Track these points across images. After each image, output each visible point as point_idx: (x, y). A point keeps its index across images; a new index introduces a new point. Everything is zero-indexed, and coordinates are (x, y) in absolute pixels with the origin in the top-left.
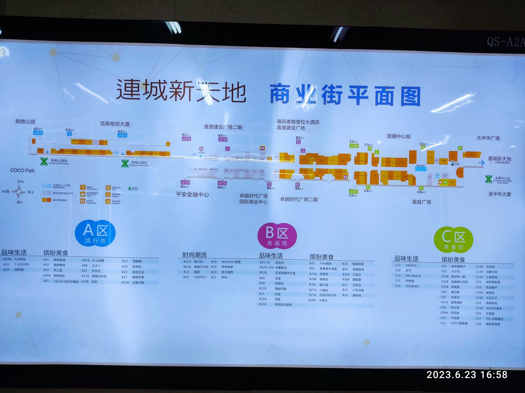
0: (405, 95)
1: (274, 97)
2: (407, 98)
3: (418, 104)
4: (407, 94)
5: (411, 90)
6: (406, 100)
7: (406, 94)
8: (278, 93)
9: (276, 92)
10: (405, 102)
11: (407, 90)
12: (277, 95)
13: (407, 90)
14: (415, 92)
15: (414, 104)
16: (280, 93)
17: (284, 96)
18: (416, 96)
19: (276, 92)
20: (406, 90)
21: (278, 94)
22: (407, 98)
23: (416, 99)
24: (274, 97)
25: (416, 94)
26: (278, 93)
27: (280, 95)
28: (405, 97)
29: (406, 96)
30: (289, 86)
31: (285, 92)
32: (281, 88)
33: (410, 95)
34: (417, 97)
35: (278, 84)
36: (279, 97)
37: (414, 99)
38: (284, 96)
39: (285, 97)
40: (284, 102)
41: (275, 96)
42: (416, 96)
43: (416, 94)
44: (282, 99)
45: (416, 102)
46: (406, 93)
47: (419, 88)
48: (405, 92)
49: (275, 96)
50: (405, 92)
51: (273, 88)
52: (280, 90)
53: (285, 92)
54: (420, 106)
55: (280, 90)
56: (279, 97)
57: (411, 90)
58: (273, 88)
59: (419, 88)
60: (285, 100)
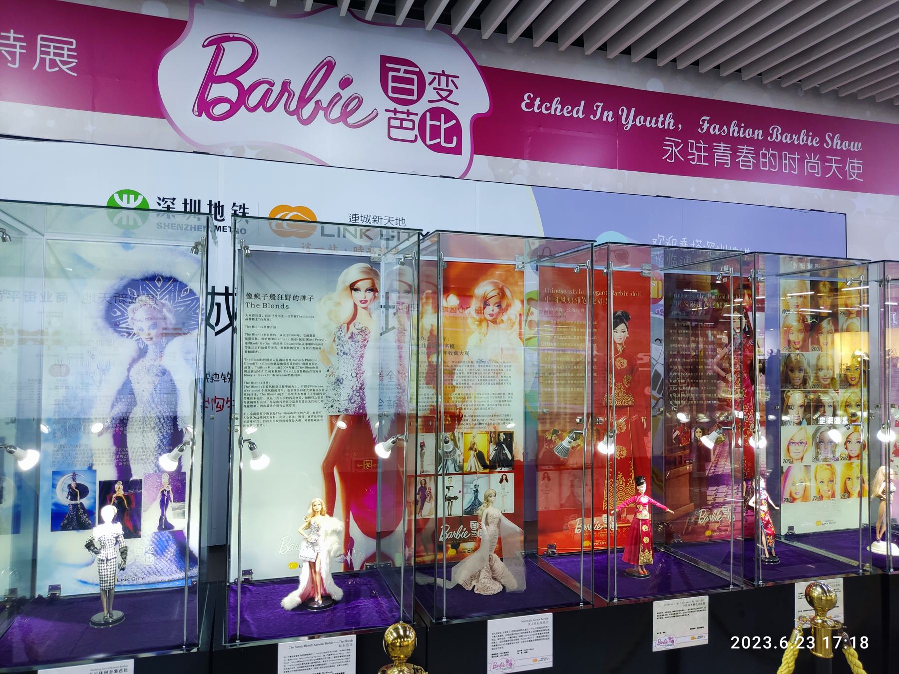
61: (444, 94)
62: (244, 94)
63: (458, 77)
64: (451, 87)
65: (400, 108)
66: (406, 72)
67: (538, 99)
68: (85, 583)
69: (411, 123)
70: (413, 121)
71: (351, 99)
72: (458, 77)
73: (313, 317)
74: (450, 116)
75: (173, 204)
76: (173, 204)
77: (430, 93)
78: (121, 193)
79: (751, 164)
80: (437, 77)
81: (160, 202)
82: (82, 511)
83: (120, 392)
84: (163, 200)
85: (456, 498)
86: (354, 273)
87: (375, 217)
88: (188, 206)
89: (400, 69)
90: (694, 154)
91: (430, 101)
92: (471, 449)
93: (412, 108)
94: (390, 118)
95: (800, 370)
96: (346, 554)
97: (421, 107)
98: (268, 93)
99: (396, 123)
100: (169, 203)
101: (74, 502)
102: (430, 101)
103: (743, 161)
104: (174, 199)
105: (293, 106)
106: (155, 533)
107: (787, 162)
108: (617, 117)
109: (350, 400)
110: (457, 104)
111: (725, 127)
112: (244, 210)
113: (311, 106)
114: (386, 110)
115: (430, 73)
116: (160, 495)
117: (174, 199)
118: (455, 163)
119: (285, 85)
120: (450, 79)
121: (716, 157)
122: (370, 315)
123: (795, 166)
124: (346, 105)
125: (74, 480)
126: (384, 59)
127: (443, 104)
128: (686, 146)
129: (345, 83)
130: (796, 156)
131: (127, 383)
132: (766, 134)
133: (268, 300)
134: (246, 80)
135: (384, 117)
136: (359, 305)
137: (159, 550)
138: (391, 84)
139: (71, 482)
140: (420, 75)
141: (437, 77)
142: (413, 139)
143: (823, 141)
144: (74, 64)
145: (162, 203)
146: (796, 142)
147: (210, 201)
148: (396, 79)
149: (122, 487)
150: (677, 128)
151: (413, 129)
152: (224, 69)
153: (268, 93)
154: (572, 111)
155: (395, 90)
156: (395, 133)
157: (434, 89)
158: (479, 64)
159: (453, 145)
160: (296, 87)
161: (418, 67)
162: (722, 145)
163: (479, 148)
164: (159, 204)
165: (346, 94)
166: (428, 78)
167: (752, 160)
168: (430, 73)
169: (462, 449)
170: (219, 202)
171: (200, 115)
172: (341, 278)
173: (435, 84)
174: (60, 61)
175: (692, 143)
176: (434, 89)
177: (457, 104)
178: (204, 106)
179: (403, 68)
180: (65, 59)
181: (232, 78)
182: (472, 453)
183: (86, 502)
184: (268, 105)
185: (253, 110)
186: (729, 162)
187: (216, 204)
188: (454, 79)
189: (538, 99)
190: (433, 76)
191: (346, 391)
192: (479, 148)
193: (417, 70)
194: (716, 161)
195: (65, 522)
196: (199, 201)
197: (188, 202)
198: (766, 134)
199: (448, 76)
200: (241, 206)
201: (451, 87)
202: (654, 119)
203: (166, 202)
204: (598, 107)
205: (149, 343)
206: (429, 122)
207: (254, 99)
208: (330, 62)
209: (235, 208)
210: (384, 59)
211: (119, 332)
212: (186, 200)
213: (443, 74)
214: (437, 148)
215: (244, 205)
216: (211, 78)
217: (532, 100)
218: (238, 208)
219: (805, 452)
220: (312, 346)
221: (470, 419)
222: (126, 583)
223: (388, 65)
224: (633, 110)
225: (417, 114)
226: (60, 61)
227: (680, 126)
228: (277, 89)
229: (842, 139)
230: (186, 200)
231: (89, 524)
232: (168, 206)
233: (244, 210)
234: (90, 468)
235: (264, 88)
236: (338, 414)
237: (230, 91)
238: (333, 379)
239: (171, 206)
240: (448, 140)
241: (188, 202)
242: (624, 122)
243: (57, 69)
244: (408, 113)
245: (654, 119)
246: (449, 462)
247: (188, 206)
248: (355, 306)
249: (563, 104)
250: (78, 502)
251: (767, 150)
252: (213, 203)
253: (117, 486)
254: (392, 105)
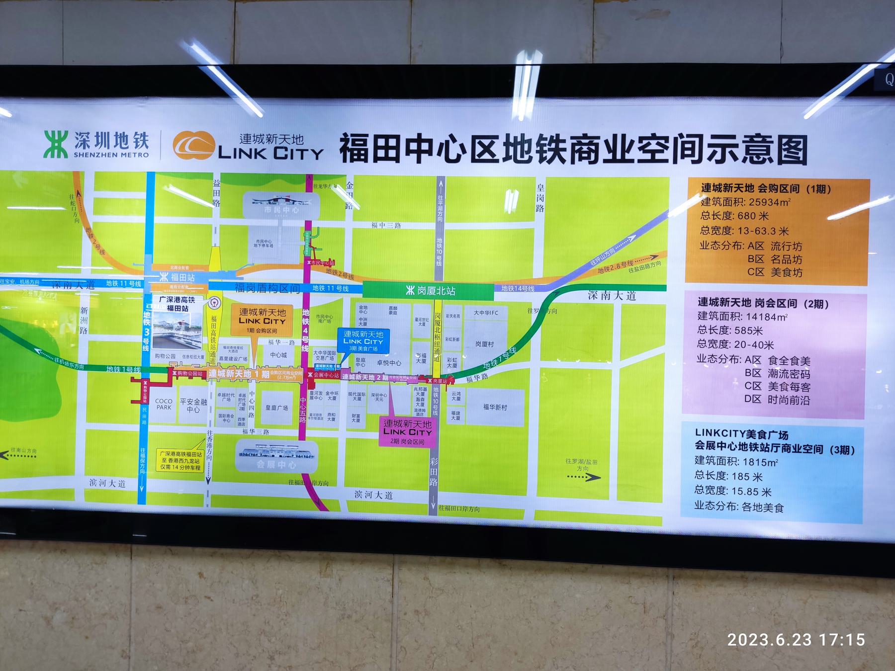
0: (783, 147)
1: (577, 155)
2: (786, 152)
3: (804, 162)
4: (787, 147)
5: (794, 140)
6: (785, 156)
7: (785, 146)
8: (583, 148)
9: (580, 147)
10: (784, 159)
11: (787, 140)
12: (580, 151)
13: (787, 140)
14: (799, 143)
15: (797, 161)
16: (585, 148)
17: (592, 153)
18: (800, 150)
19: (580, 147)
20: (784, 141)
21: (583, 150)
22: (786, 152)
23: (801, 154)
24: (577, 155)
25: (801, 146)
26: (583, 148)
27: (585, 152)
28: (784, 151)
29: (785, 150)
30: (600, 137)
31: (593, 147)
32: (587, 141)
33: (791, 147)
34: (802, 151)
35: (582, 135)
36: (585, 155)
37: (798, 153)
38: (592, 153)
39: (593, 155)
40: (590, 163)
41: (578, 154)
42: (800, 150)
43: (801, 146)
44: (589, 158)
45: (801, 159)
46: (785, 145)
47: (805, 138)
48: (783, 143)
49: (578, 154)
50: (783, 143)
51: (575, 141)
52: (585, 144)
53: (593, 147)
54: (806, 165)
55: (585, 144)
56: (585, 155)
57: (794, 140)
58: (575, 141)
59: (805, 138)
60: (593, 158)
75: (88, 138)
76: (88, 138)
81: (78, 136)
84: (80, 135)
87: (269, 136)
88: (100, 138)
104: (88, 133)
112: (144, 138)
117: (88, 133)
147: (117, 133)
164: (77, 139)
170: (124, 133)
187: (121, 134)
196: (108, 133)
197: (100, 134)
200: (141, 134)
203: (82, 136)
209: (137, 137)
212: (97, 133)
215: (144, 133)
218: (139, 137)
230: (97, 133)
232: (84, 139)
233: (144, 138)
239: (87, 139)
241: (100, 134)
247: (100, 138)
252: (119, 134)
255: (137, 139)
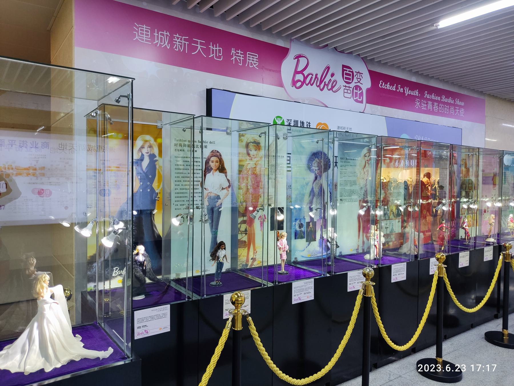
61: (359, 80)
62: (305, 78)
63: (363, 74)
64: (361, 78)
65: (348, 85)
66: (349, 71)
67: (384, 83)
68: (303, 257)
69: (350, 91)
70: (350, 90)
71: (334, 81)
72: (363, 74)
73: (355, 166)
74: (360, 89)
77: (355, 80)
78: (277, 117)
79: (437, 110)
80: (357, 73)
81: (287, 121)
82: (302, 232)
83: (311, 192)
85: (388, 228)
86: (365, 151)
89: (347, 70)
90: (423, 105)
91: (355, 83)
92: (391, 211)
93: (350, 85)
94: (344, 89)
95: (465, 184)
96: (363, 247)
97: (352, 85)
98: (312, 78)
99: (346, 91)
100: (290, 122)
101: (300, 229)
102: (355, 83)
103: (435, 108)
104: (291, 120)
105: (318, 84)
106: (319, 239)
107: (441, 108)
108: (404, 90)
109: (364, 194)
110: (362, 84)
111: (431, 96)
113: (323, 84)
114: (343, 86)
115: (355, 72)
116: (320, 226)
117: (291, 120)
118: (361, 106)
119: (316, 75)
120: (361, 74)
121: (428, 107)
122: (369, 165)
123: (448, 111)
124: (333, 84)
125: (300, 222)
126: (344, 66)
127: (358, 84)
128: (421, 102)
129: (333, 75)
130: (448, 107)
131: (313, 188)
132: (441, 99)
133: (345, 160)
134: (306, 73)
135: (343, 88)
136: (367, 162)
137: (321, 245)
138: (345, 76)
139: (299, 222)
140: (352, 72)
141: (357, 73)
142: (350, 97)
143: (455, 102)
144: (257, 64)
145: (288, 121)
146: (448, 102)
148: (347, 74)
149: (311, 224)
150: (419, 95)
151: (350, 93)
152: (299, 69)
153: (312, 78)
154: (392, 88)
155: (346, 78)
156: (346, 95)
157: (357, 78)
158: (369, 69)
159: (361, 100)
160: (319, 76)
161: (352, 69)
162: (430, 102)
163: (368, 102)
165: (333, 79)
166: (355, 74)
167: (437, 108)
168: (355, 72)
169: (390, 211)
171: (293, 87)
172: (362, 153)
173: (357, 76)
174: (253, 63)
175: (422, 101)
176: (357, 78)
177: (362, 84)
178: (294, 83)
179: (348, 70)
180: (255, 62)
181: (301, 72)
182: (392, 212)
183: (303, 229)
184: (312, 83)
185: (307, 85)
186: (431, 108)
188: (361, 74)
189: (384, 83)
190: (356, 73)
191: (363, 191)
192: (368, 102)
193: (352, 70)
194: (428, 108)
195: (298, 236)
197: (295, 121)
198: (441, 99)
199: (360, 73)
201: (361, 78)
202: (413, 92)
204: (399, 86)
205: (318, 175)
206: (355, 91)
207: (308, 81)
208: (329, 66)
210: (344, 66)
211: (310, 171)
212: (294, 120)
213: (359, 72)
214: (356, 101)
216: (296, 72)
217: (382, 83)
219: (465, 211)
220: (355, 176)
221: (391, 201)
222: (312, 256)
223: (344, 69)
224: (408, 88)
225: (351, 88)
226: (253, 63)
227: (420, 95)
228: (314, 77)
229: (460, 101)
230: (294, 120)
231: (304, 237)
234: (304, 217)
235: (310, 76)
236: (361, 199)
237: (300, 77)
238: (360, 187)
239: (290, 123)
240: (360, 98)
241: (295, 121)
242: (406, 93)
243: (253, 66)
244: (349, 87)
245: (413, 92)
246: (387, 216)
248: (365, 162)
249: (390, 85)
250: (301, 229)
251: (441, 104)
253: (310, 224)
254: (345, 84)
255: (307, 124)
